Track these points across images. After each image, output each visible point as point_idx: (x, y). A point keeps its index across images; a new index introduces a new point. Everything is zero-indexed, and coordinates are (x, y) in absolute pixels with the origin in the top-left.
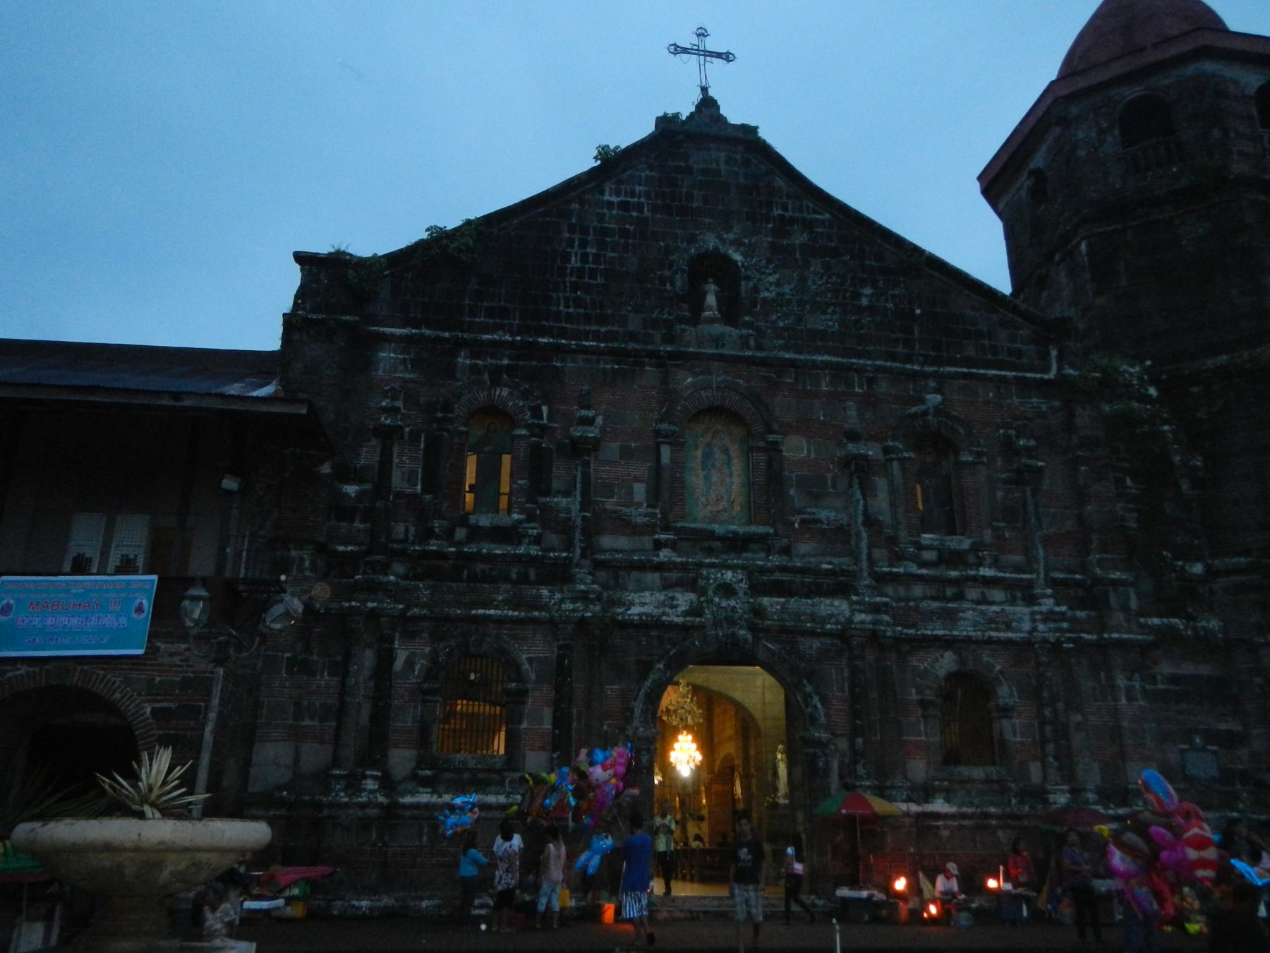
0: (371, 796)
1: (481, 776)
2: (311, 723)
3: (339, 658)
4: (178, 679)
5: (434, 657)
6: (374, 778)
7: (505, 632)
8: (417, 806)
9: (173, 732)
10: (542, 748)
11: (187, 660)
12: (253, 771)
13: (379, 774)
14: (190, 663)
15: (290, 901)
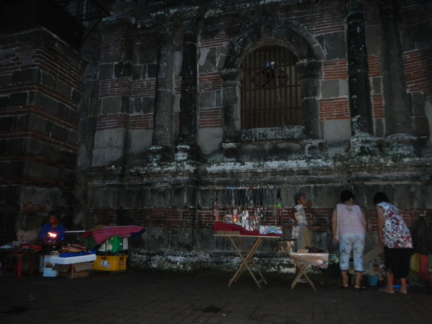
0: (179, 165)
1: (282, 145)
2: (138, 114)
3: (155, 62)
4: (12, 74)
5: (231, 51)
6: (185, 150)
7: (294, 17)
8: (223, 174)
9: (8, 116)
10: (340, 117)
11: (17, 59)
12: (95, 152)
13: (188, 147)
14: (20, 61)
15: (104, 255)
